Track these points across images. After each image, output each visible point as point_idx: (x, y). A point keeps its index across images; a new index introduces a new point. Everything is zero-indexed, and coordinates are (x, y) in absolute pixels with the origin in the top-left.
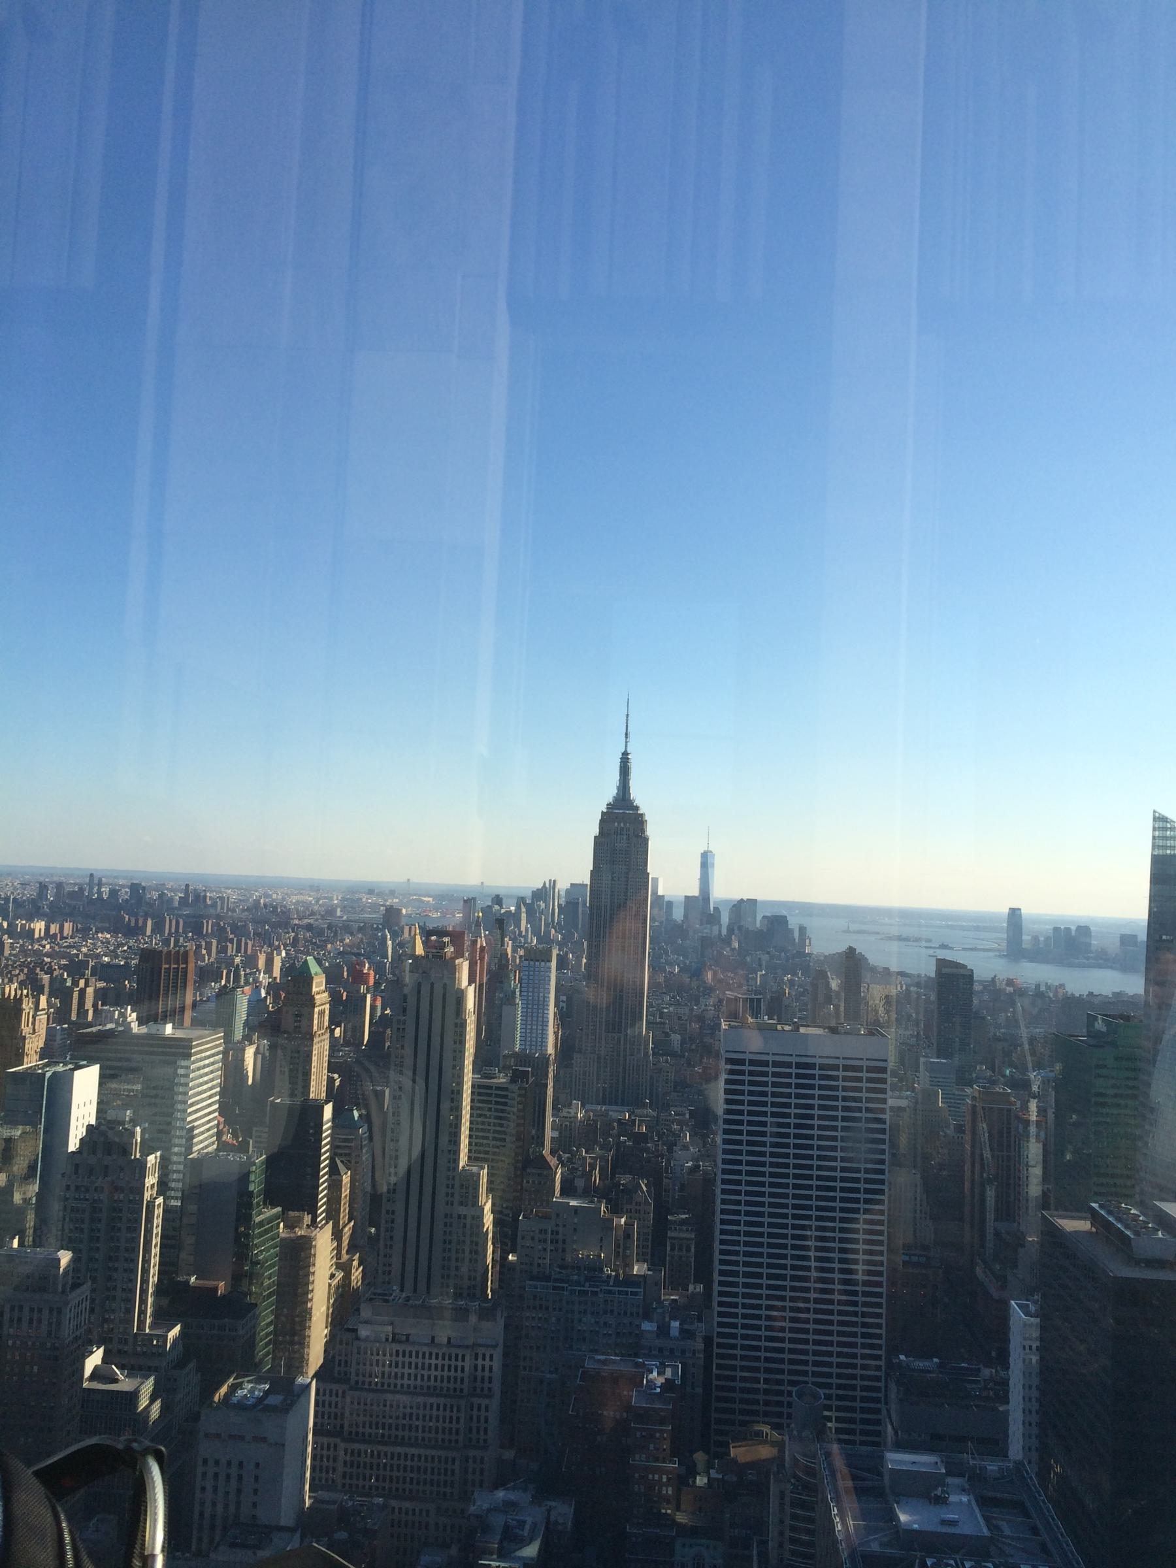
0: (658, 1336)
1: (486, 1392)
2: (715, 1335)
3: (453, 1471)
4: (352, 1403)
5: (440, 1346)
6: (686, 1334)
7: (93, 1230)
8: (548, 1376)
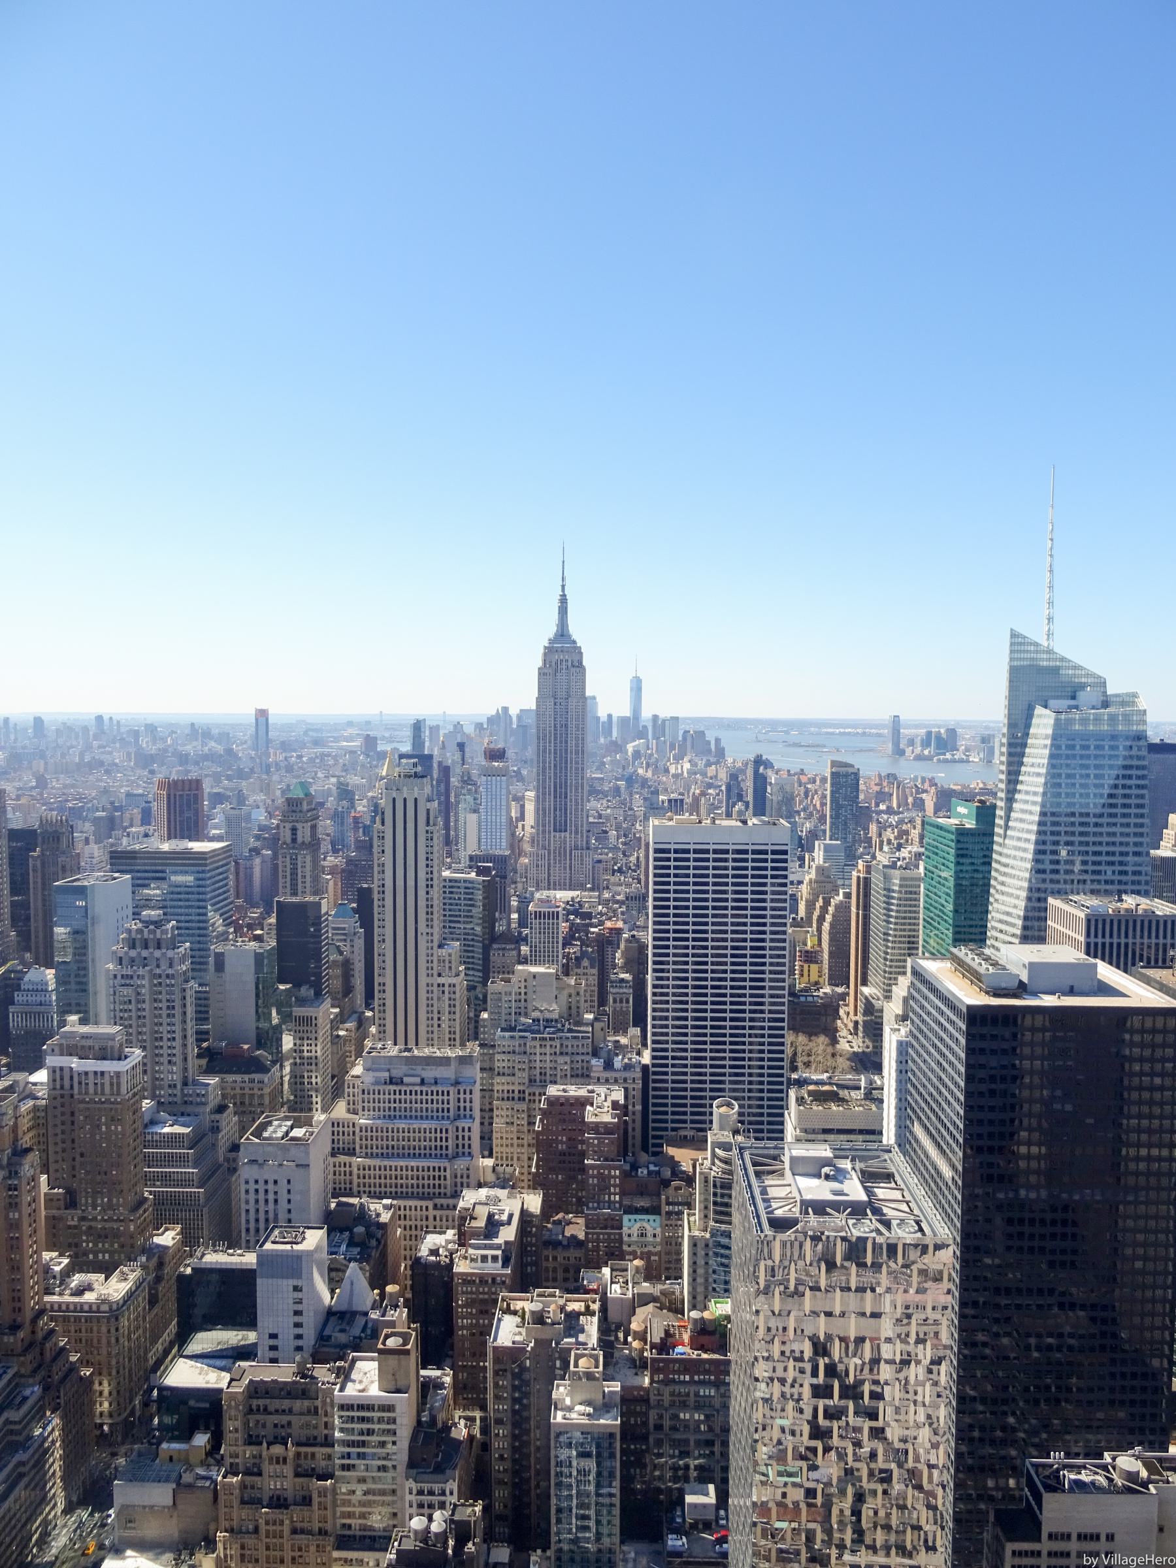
0: (605, 1068)
3: (445, 1179)
7: (139, 1010)
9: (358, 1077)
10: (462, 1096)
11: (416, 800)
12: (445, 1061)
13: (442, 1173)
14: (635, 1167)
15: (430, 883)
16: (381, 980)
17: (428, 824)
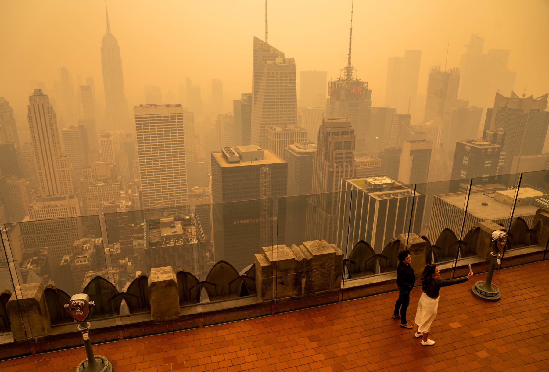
3: (69, 236)
6: (133, 192)
9: (32, 207)
10: (72, 209)
11: (42, 104)
13: (68, 235)
14: (136, 225)
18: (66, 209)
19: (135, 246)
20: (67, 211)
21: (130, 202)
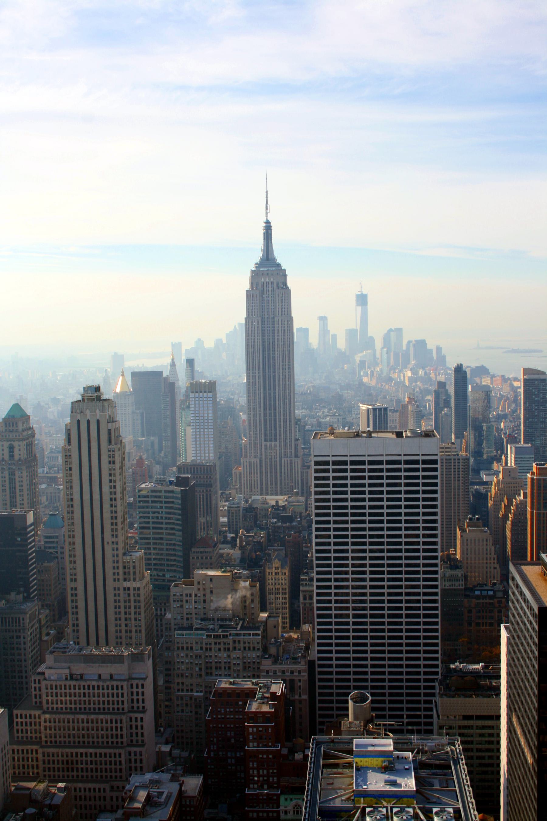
1: (141, 709)
2: (316, 660)
3: (120, 762)
4: (45, 722)
5: (105, 681)
8: (195, 694)
9: (43, 673)
10: (135, 690)
11: (98, 421)
12: (119, 659)
13: (118, 759)
14: (292, 751)
15: (113, 496)
16: (73, 585)
17: (110, 442)
18: (122, 687)
19: (286, 812)
20: (122, 694)
21: (282, 685)
